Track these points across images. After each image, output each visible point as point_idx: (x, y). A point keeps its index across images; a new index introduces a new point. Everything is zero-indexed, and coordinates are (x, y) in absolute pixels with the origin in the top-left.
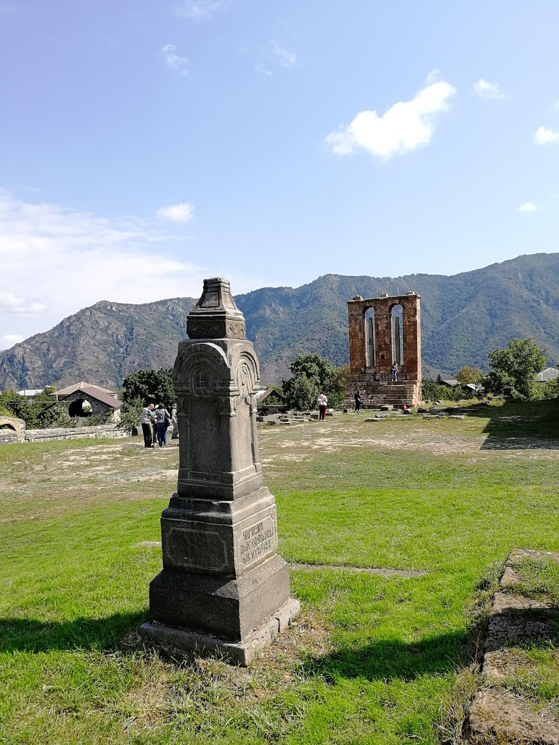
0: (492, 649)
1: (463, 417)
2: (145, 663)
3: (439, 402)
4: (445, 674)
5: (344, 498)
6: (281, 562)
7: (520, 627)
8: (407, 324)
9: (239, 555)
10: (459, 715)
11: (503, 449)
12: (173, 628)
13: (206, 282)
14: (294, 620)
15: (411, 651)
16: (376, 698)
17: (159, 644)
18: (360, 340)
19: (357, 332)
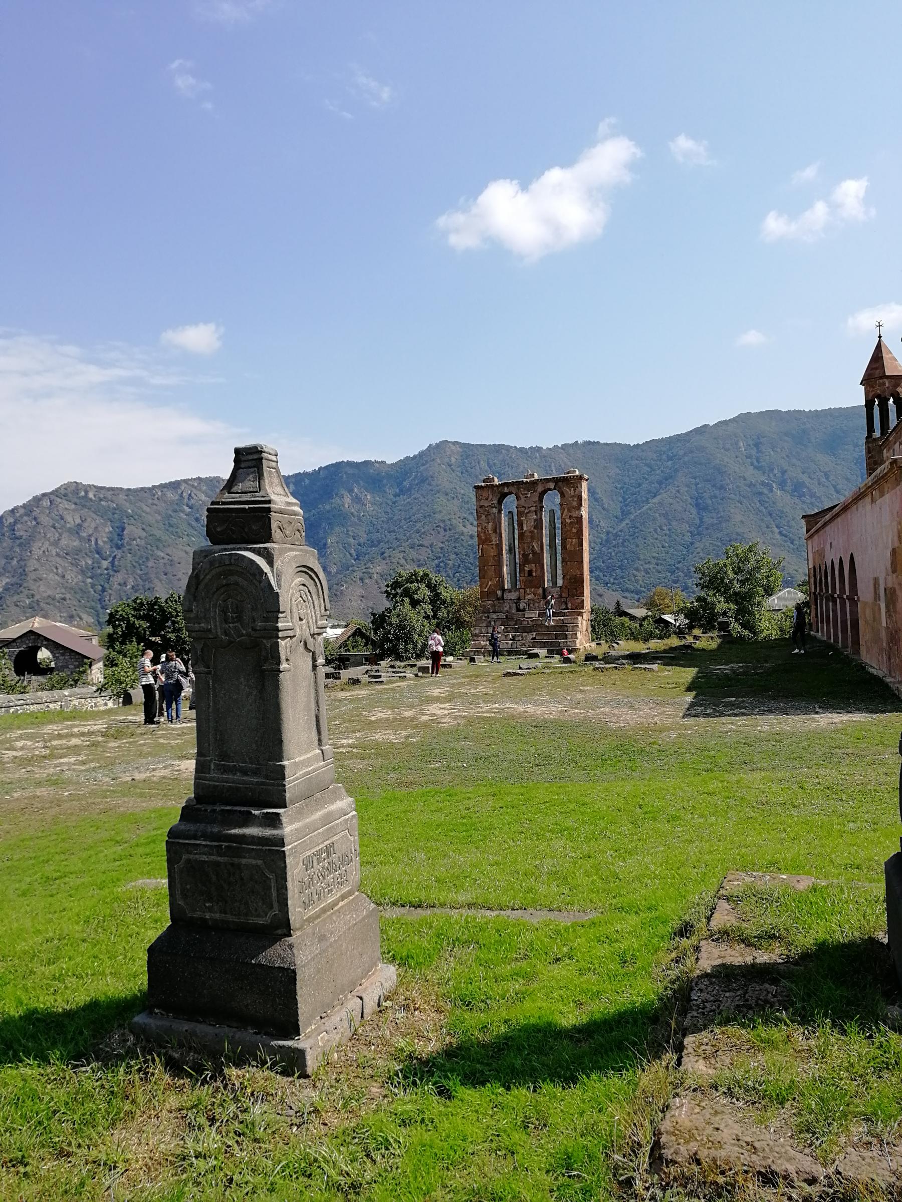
0: (696, 1030)
2: (141, 1079)
3: (618, 644)
4: (624, 1072)
5: (469, 799)
6: (366, 904)
7: (739, 993)
8: (568, 521)
9: (297, 896)
10: (645, 1137)
11: (717, 716)
12: (188, 1020)
13: (237, 451)
14: (387, 998)
15: (571, 1038)
16: (517, 1116)
17: (165, 1047)
18: (494, 547)
19: (490, 535)
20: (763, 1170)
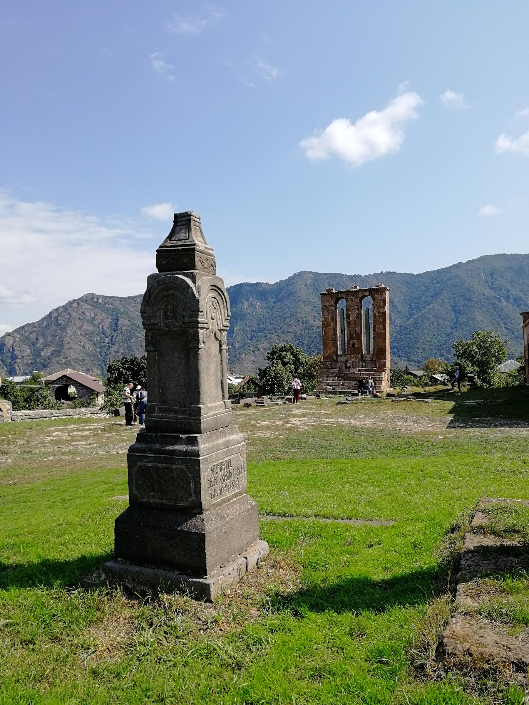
0: (465, 581)
1: (429, 400)
2: (108, 600)
3: (406, 388)
4: (416, 605)
5: (316, 465)
6: (250, 501)
7: (492, 562)
8: (377, 314)
9: (206, 489)
10: (432, 640)
11: (468, 428)
12: (138, 565)
13: (176, 216)
14: (263, 560)
15: (381, 587)
16: (345, 628)
17: (124, 581)
18: (332, 329)
19: (329, 322)
20: (516, 661)
